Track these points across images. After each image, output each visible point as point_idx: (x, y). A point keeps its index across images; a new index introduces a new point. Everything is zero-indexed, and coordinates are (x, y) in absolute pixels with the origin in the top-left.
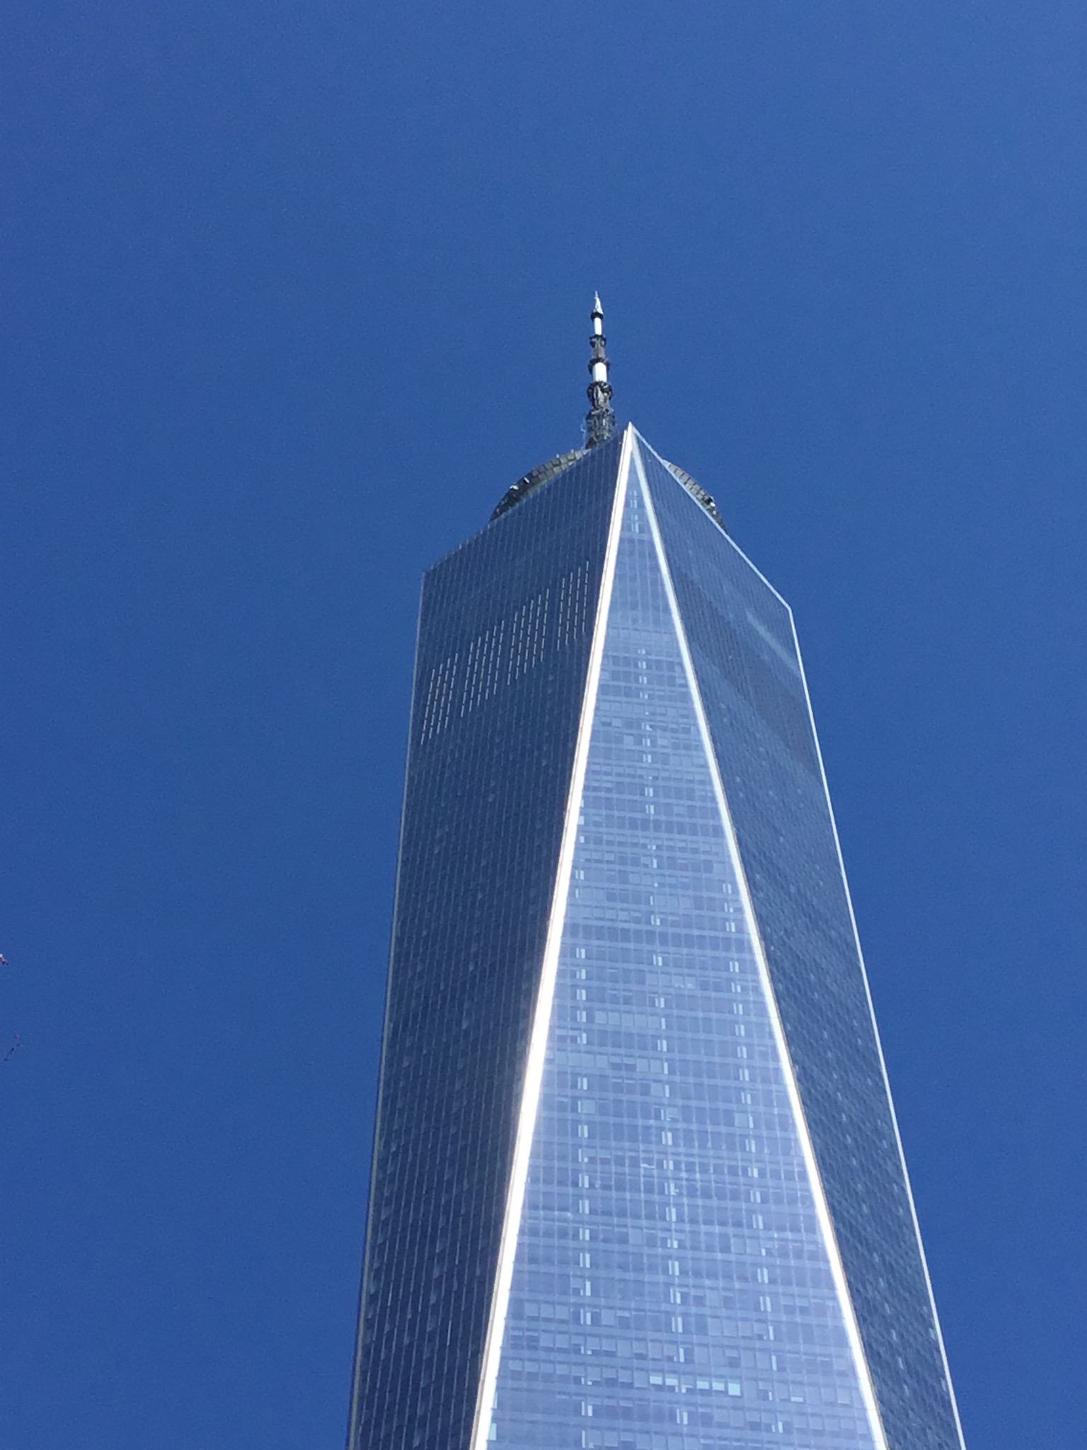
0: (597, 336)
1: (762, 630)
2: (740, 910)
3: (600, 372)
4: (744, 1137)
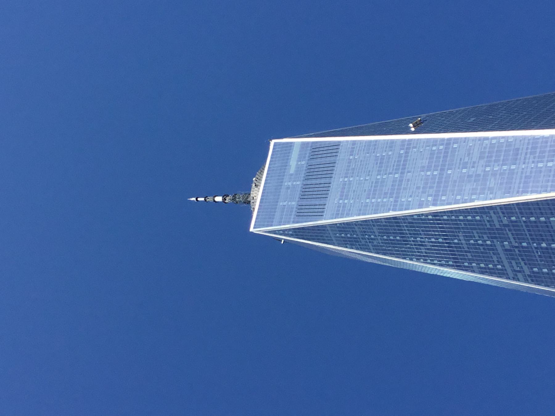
0: (205, 200)
1: (293, 163)
2: (422, 215)
3: (219, 199)
4: (512, 222)
